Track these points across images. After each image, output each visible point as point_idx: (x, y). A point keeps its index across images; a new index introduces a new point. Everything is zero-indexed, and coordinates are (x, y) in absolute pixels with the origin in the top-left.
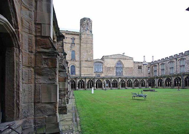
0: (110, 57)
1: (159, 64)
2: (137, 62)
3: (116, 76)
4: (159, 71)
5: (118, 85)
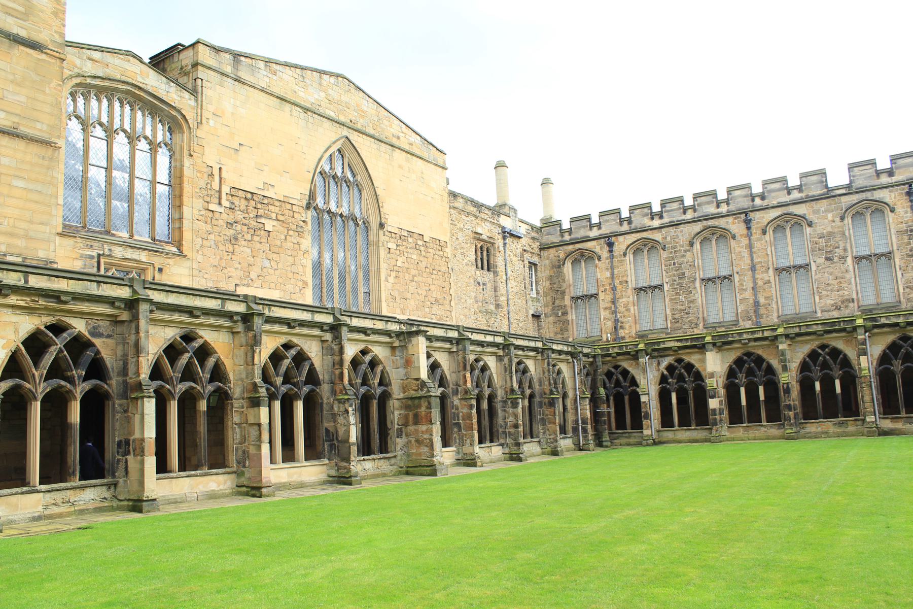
0: (285, 82)
1: (610, 245)
4: (614, 302)
5: (395, 415)
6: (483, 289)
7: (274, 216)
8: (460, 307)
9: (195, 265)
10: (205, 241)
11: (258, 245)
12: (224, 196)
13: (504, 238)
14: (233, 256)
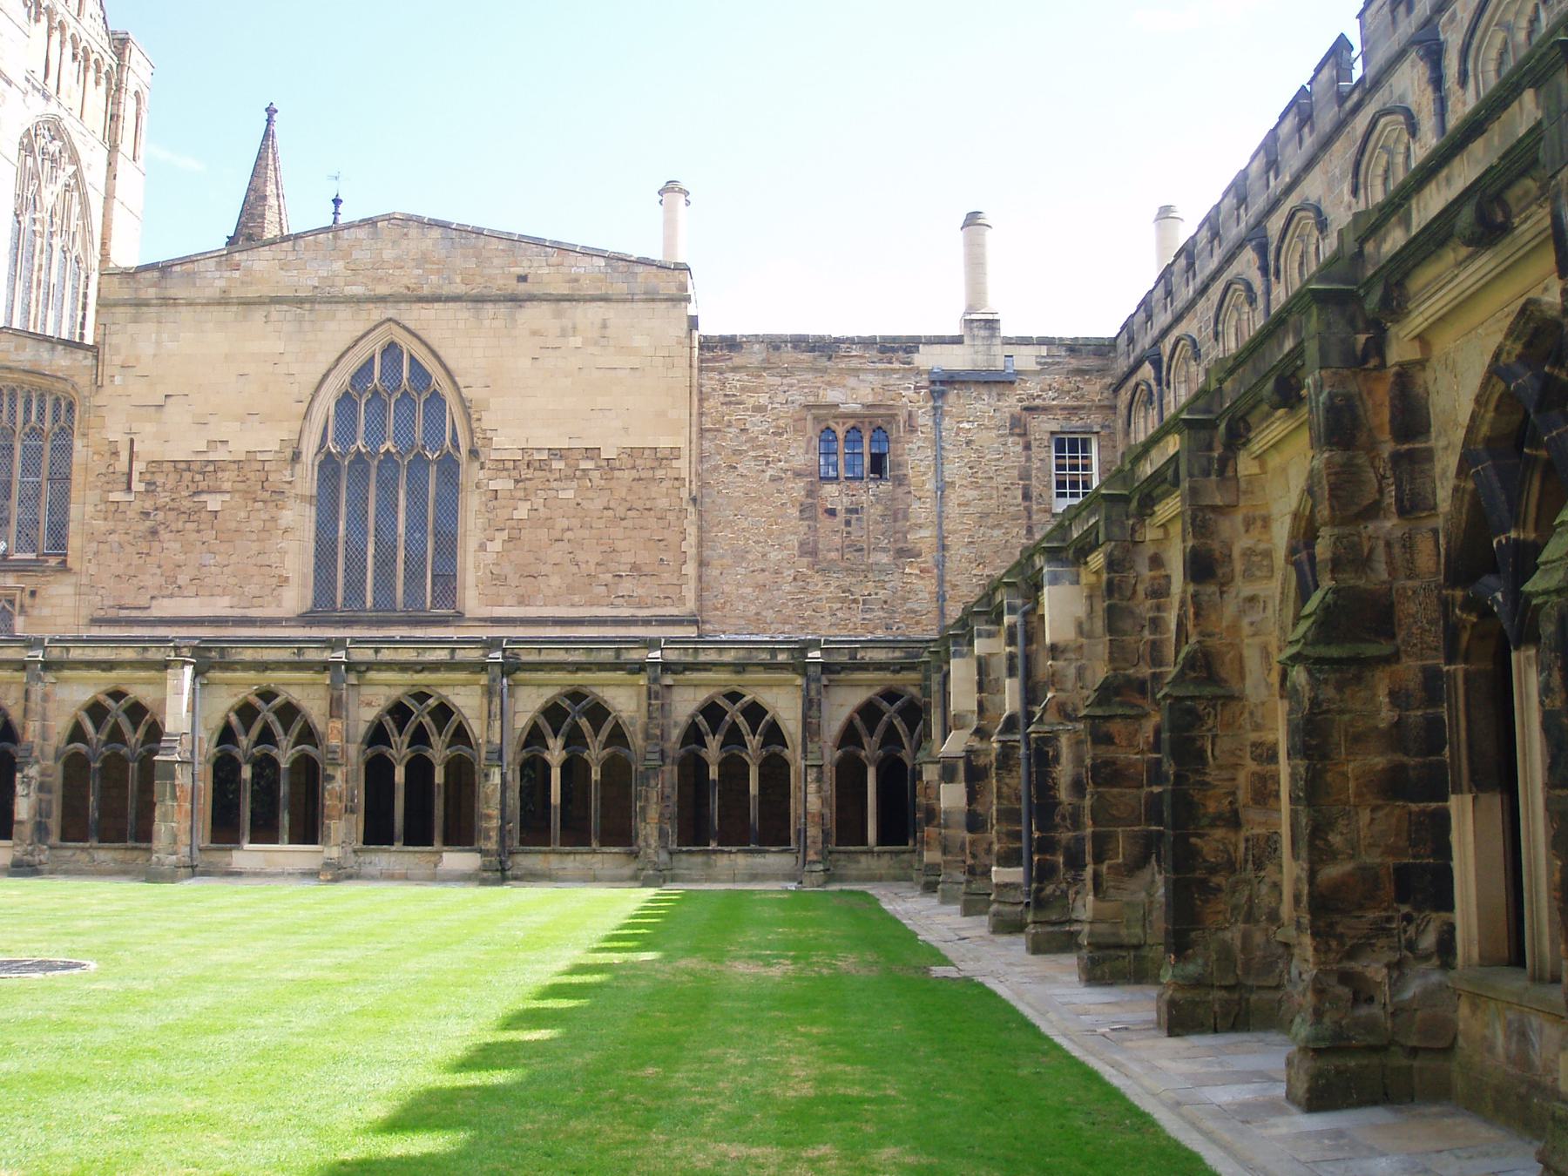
2: (774, 344)
3: (306, 619)
6: (848, 523)
7: (227, 486)
8: (743, 571)
9: (84, 580)
10: (101, 545)
11: (195, 535)
12: (135, 476)
13: (938, 396)
14: (148, 559)
